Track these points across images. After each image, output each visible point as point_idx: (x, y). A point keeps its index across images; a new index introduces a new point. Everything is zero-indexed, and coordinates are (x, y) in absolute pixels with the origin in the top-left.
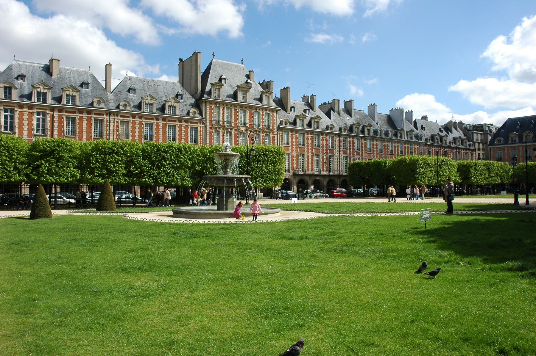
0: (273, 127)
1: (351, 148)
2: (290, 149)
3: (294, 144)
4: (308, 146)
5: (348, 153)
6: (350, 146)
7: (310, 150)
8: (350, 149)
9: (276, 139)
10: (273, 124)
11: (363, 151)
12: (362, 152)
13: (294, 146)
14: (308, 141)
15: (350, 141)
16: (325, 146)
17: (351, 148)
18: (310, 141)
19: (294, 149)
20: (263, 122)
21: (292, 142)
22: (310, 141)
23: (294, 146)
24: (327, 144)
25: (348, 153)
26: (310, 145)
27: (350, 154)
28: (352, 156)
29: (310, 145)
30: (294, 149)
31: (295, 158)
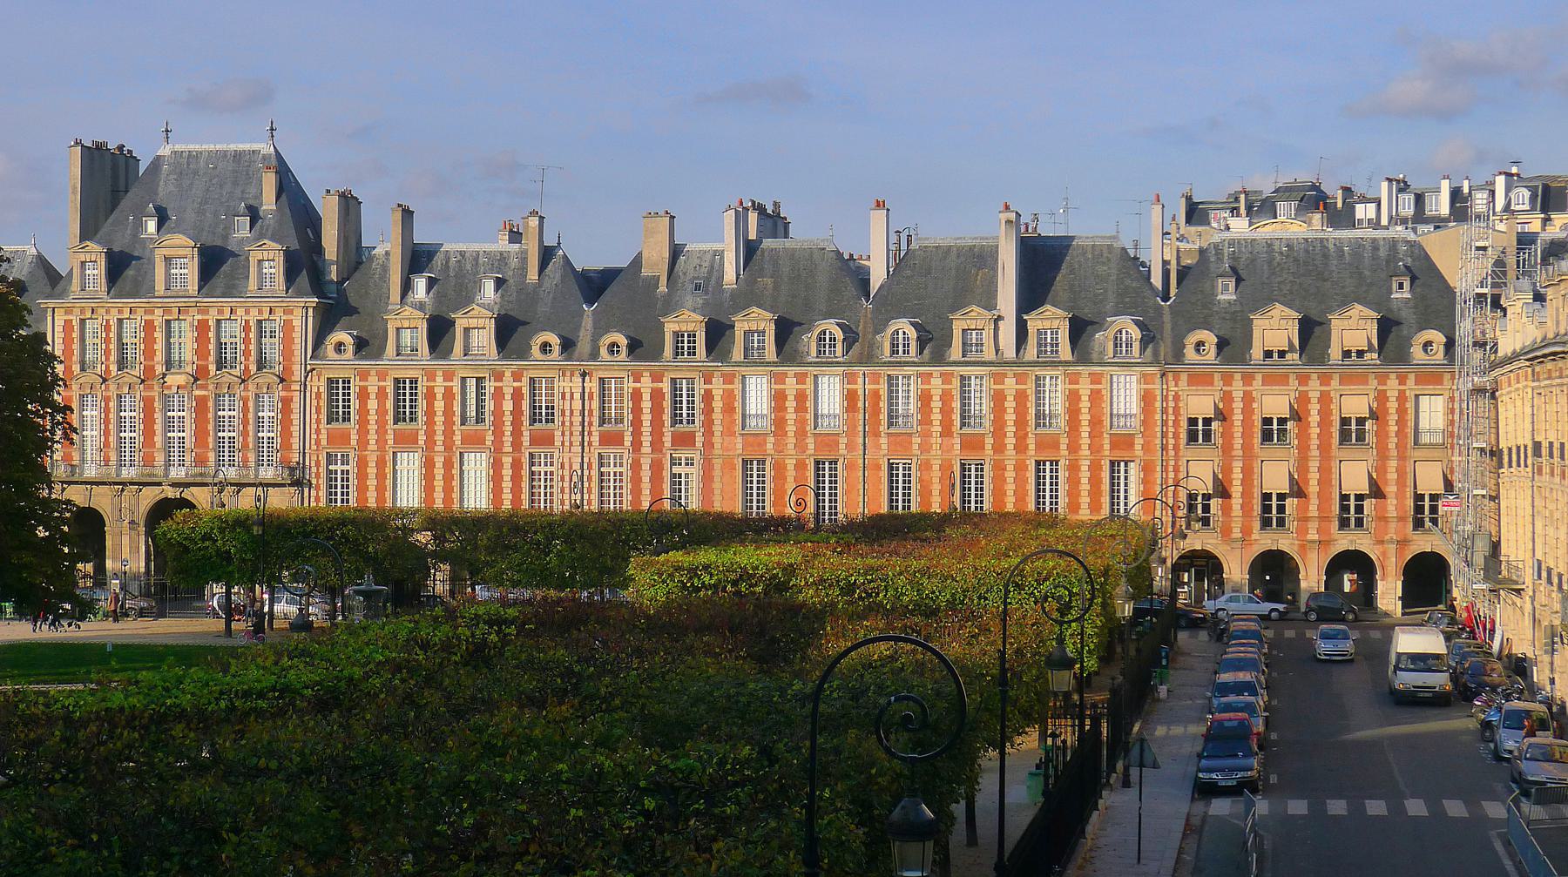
0: (288, 369)
1: (646, 418)
2: (354, 437)
3: (373, 418)
4: (430, 422)
5: (628, 439)
6: (637, 410)
7: (439, 438)
8: (637, 424)
9: (295, 406)
10: (287, 354)
11: (717, 428)
12: (709, 432)
13: (373, 427)
14: (430, 405)
15: (636, 396)
16: (508, 418)
17: (646, 418)
18: (439, 405)
19: (372, 438)
20: (247, 353)
21: (364, 411)
22: (439, 405)
23: (373, 427)
24: (517, 412)
25: (628, 439)
26: (439, 419)
27: (637, 445)
28: (646, 448)
29: (439, 419)
30: (372, 438)
31: (372, 470)
